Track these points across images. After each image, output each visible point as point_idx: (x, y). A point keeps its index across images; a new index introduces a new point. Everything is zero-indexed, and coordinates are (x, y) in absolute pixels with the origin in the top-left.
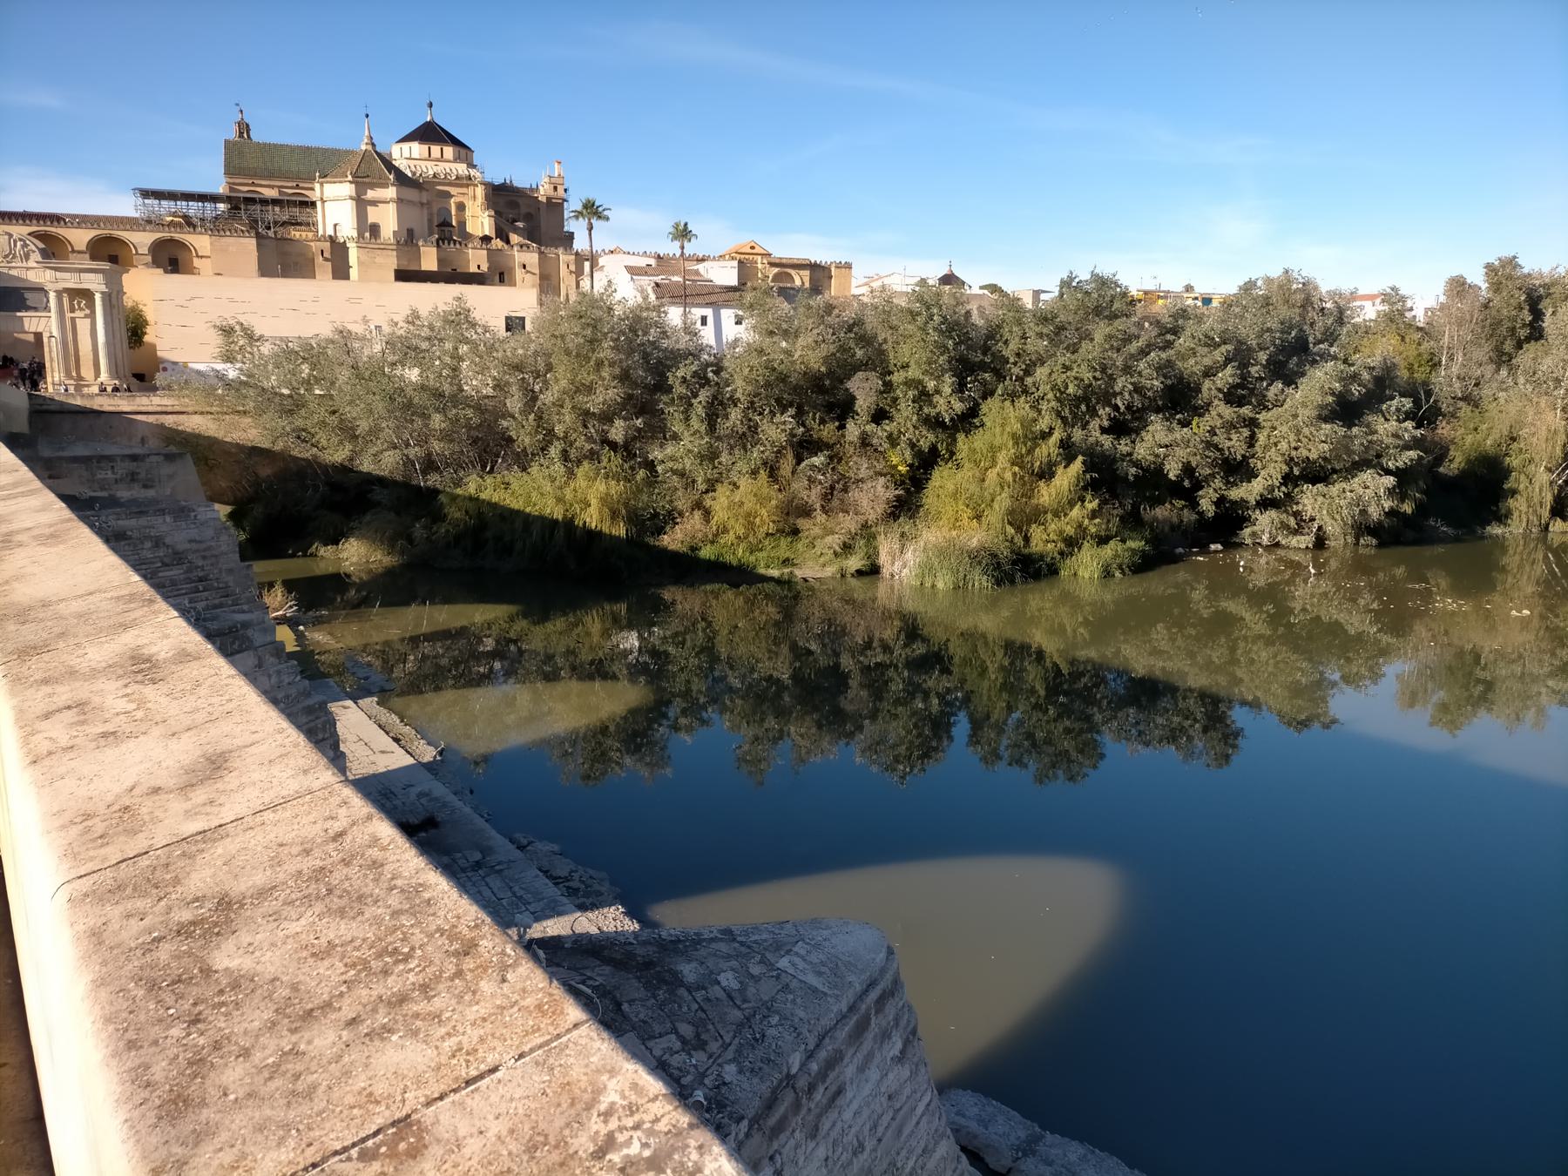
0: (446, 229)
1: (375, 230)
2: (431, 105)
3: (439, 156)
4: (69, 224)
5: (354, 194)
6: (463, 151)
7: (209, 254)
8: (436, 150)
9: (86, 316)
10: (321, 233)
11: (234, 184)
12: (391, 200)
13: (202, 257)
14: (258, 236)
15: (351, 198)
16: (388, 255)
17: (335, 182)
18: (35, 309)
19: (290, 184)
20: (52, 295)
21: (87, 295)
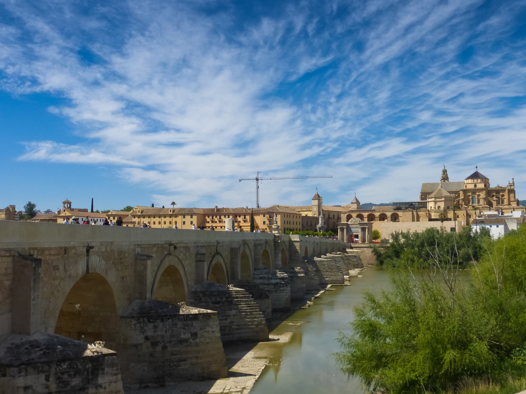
1: (439, 207)
2: (477, 167)
8: (475, 181)
10: (428, 209)
21: (365, 228)
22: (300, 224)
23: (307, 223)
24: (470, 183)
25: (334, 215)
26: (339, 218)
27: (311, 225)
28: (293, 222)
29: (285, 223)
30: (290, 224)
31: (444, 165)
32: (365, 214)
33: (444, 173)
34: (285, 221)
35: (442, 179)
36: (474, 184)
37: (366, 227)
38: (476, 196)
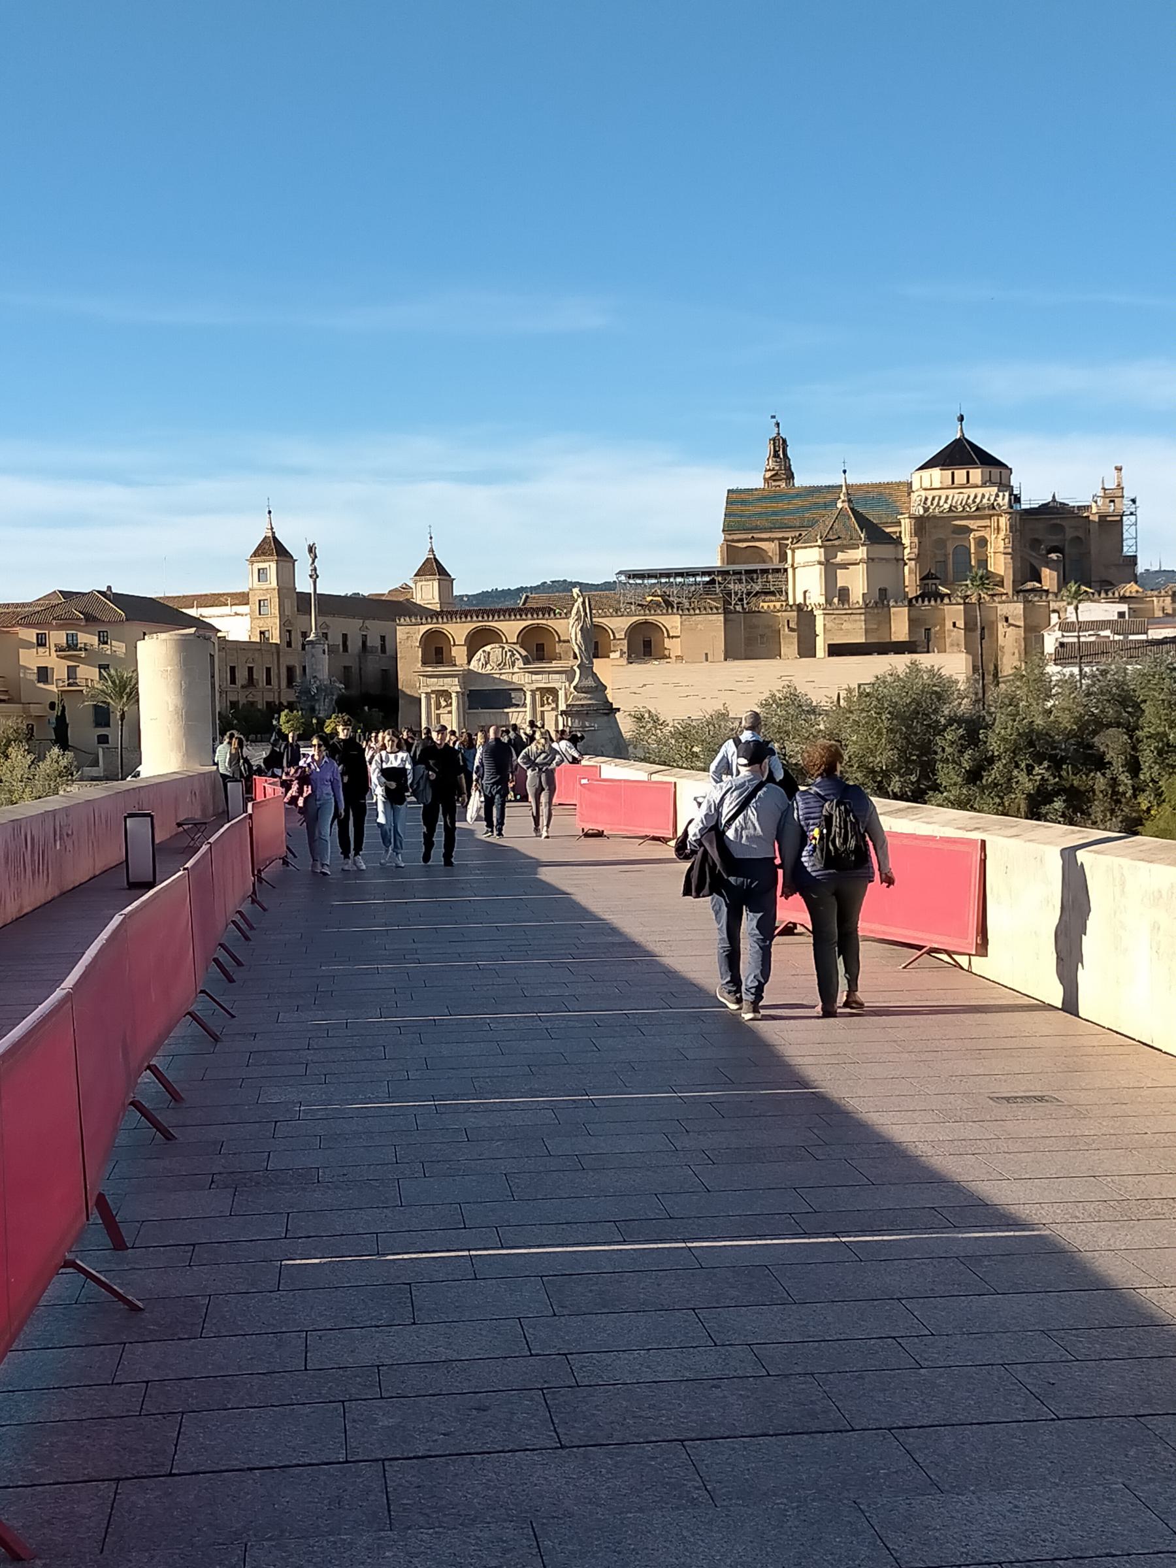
0: (930, 582)
1: (844, 594)
3: (965, 482)
4: (558, 616)
5: (823, 560)
6: (996, 471)
7: (679, 634)
8: (960, 475)
9: (553, 709)
10: (791, 603)
11: (733, 541)
12: (861, 561)
13: (673, 637)
14: (726, 612)
15: (820, 563)
16: (856, 621)
17: (806, 547)
18: (518, 706)
20: (528, 694)
23: (233, 669)
24: (939, 486)
25: (345, 636)
26: (387, 651)
27: (251, 681)
31: (774, 420)
32: (511, 628)
33: (776, 455)
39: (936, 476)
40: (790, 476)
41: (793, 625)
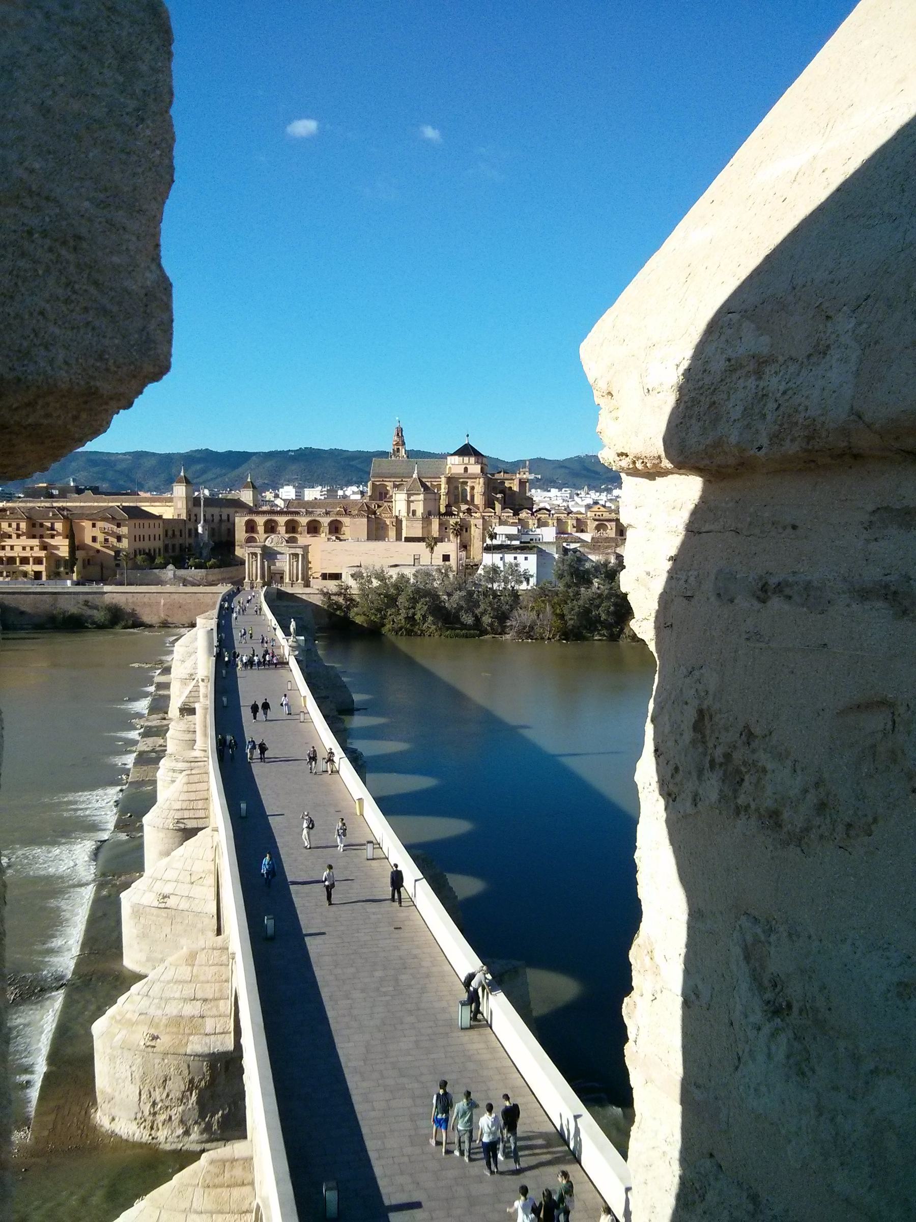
1: (414, 512)
2: (468, 436)
8: (466, 459)
10: (394, 515)
19: (399, 480)
21: (296, 555)
22: (160, 539)
25: (213, 515)
28: (149, 535)
29: (135, 541)
30: (144, 540)
32: (282, 520)
33: (398, 435)
34: (135, 536)
35: (394, 445)
36: (464, 466)
37: (299, 553)
38: (468, 489)
39: (456, 459)
40: (404, 444)
41: (394, 524)
